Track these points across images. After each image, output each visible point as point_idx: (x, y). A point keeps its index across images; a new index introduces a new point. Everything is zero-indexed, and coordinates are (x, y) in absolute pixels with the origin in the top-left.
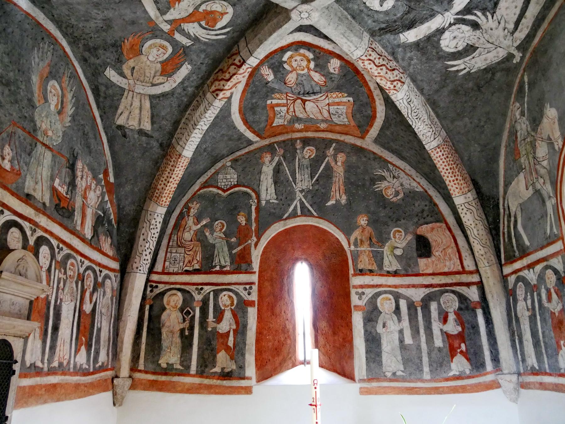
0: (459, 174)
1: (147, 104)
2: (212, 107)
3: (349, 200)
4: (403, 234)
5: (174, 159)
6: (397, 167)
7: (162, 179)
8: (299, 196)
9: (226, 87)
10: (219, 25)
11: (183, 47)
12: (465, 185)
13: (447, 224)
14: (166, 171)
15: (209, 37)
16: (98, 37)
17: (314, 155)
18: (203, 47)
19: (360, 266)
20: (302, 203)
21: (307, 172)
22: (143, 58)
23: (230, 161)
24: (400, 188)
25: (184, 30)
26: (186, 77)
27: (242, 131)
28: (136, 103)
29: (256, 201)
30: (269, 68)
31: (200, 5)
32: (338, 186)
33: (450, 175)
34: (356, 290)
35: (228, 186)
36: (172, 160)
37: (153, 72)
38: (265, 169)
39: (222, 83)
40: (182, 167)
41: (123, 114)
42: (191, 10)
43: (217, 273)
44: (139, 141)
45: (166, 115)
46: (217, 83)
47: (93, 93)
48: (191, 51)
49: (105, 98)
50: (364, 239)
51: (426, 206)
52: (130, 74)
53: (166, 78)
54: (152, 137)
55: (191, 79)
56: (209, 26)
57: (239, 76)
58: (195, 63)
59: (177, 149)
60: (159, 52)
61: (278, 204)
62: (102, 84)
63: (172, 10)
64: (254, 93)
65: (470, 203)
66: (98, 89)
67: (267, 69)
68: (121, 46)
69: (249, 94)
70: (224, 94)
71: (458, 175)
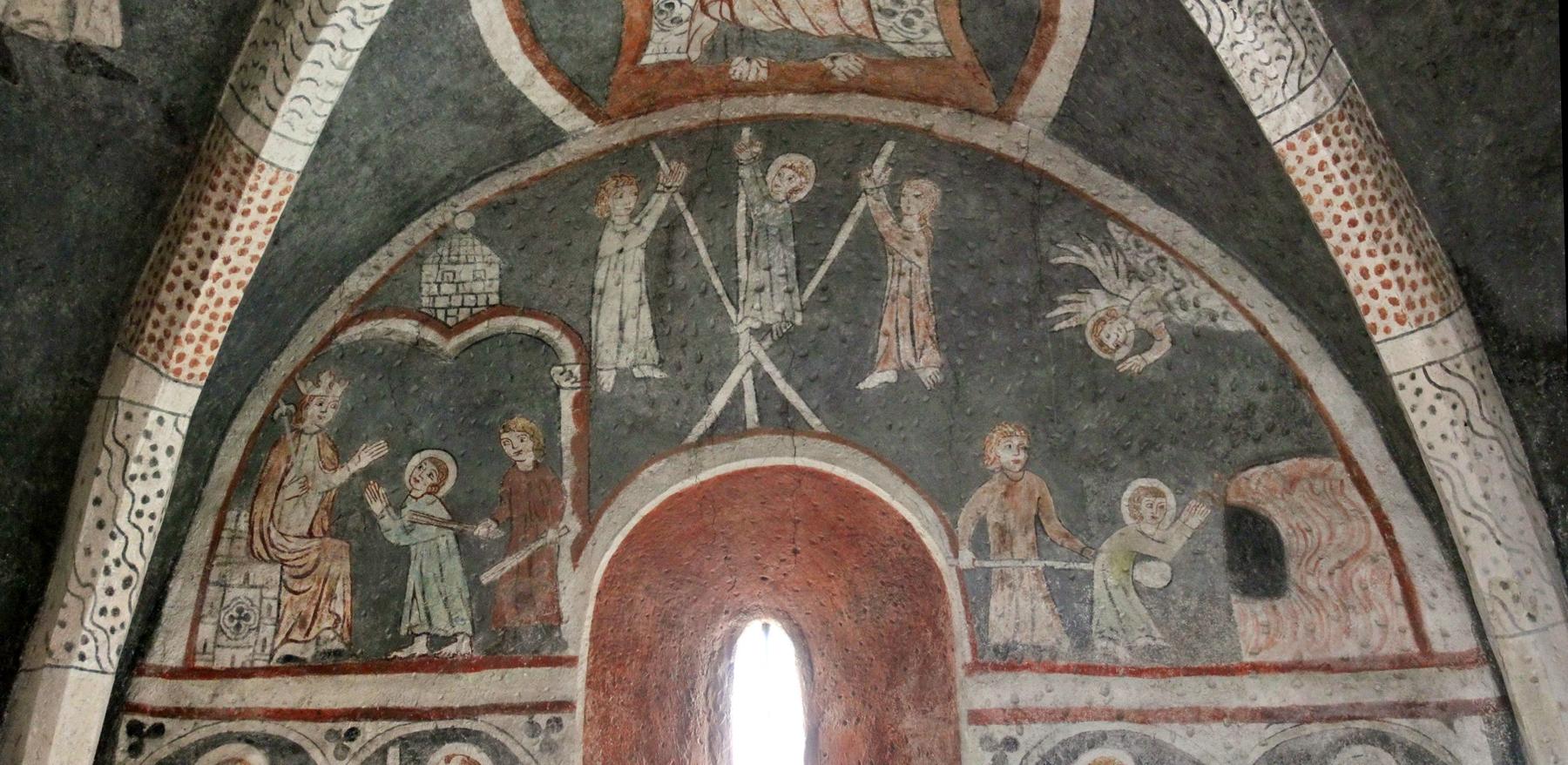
0: (1404, 243)
3: (953, 366)
4: (1171, 500)
5: (226, 175)
6: (1143, 233)
7: (176, 262)
8: (751, 352)
12: (1430, 289)
13: (1350, 463)
14: (195, 228)
17: (808, 188)
19: (1000, 631)
20: (763, 383)
21: (782, 257)
23: (469, 210)
24: (1159, 317)
27: (516, 80)
29: (577, 370)
32: (905, 312)
33: (1363, 247)
34: (981, 730)
35: (464, 314)
36: (220, 182)
38: (610, 242)
40: (262, 210)
43: (409, 666)
44: (73, 94)
50: (1012, 524)
51: (1263, 389)
59: (240, 133)
61: (664, 383)
65: (1450, 365)
71: (1398, 247)
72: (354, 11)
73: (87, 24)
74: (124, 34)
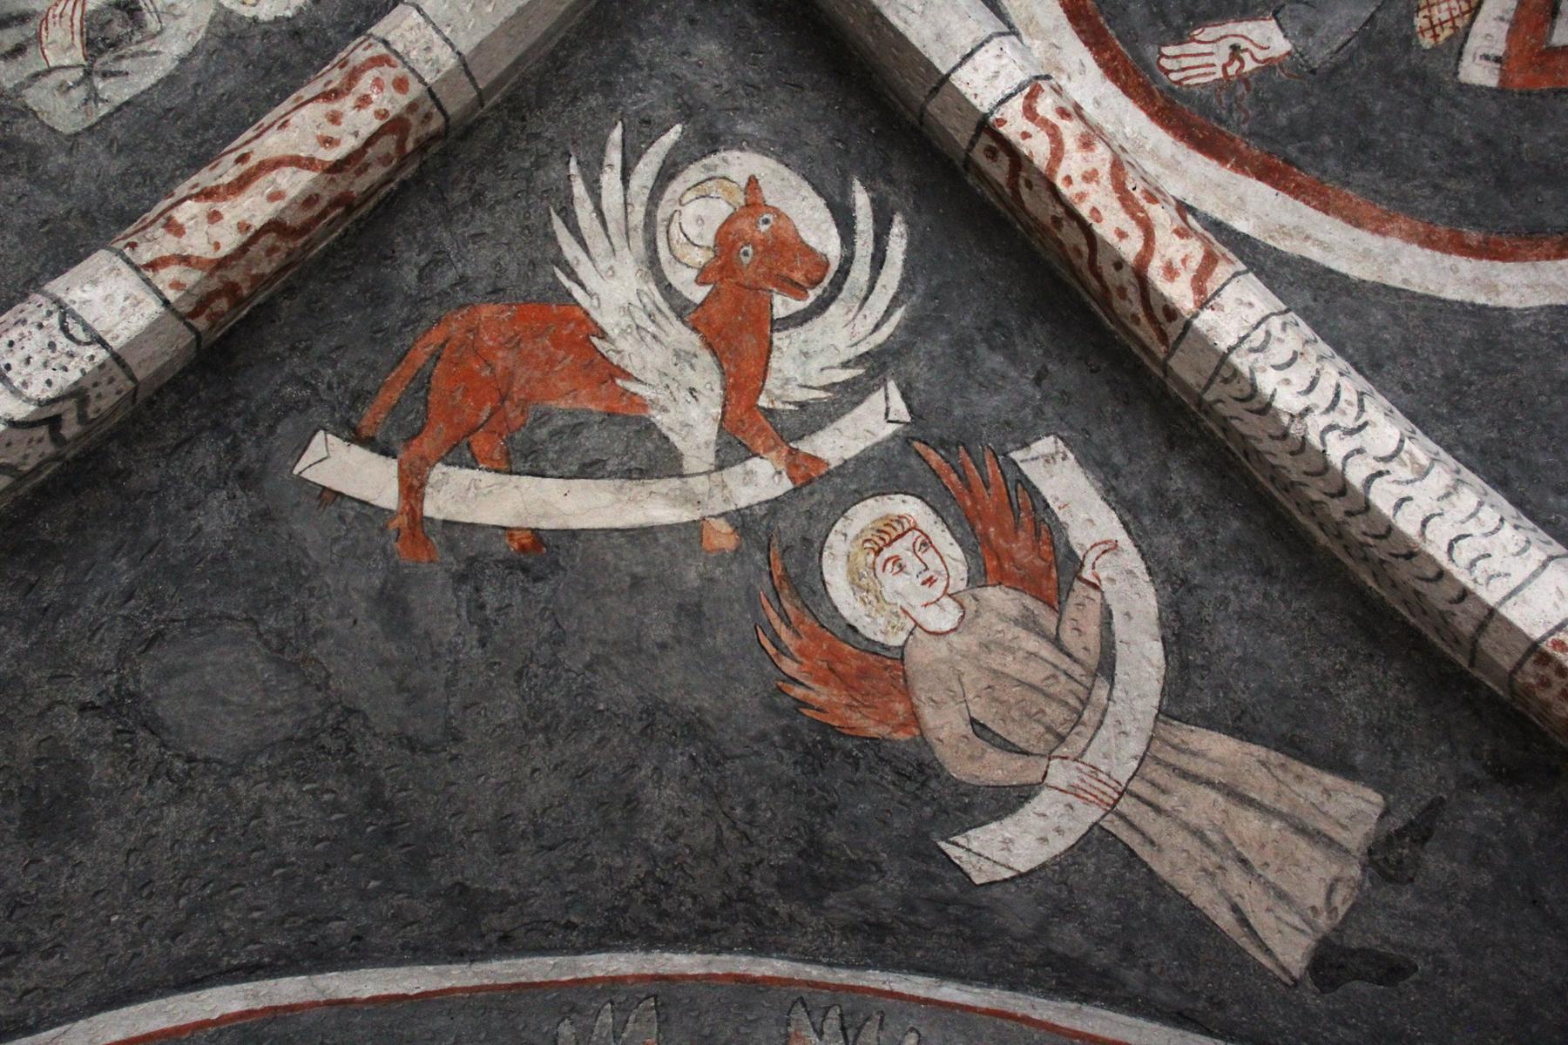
1: (1218, 747)
2: (1241, 361)
9: (1130, 248)
10: (824, 239)
11: (905, 440)
15: (880, 301)
16: (751, 806)
22: (922, 655)
25: (802, 405)
28: (1203, 806)
30: (1180, 38)
31: (667, 290)
37: (1032, 643)
39: (1108, 271)
41: (1246, 907)
42: (681, 335)
45: (1309, 668)
46: (1117, 303)
47: (1086, 998)
48: (948, 412)
49: (1128, 951)
52: (1018, 762)
54: (1434, 808)
56: (814, 284)
57: (1073, 164)
60: (912, 564)
62: (1042, 929)
63: (658, 418)
64: (1365, 147)
66: (1064, 959)
67: (1193, 48)
68: (824, 728)
69: (1359, 177)
70: (1170, 272)
73: (1344, 827)
74: (1366, 785)
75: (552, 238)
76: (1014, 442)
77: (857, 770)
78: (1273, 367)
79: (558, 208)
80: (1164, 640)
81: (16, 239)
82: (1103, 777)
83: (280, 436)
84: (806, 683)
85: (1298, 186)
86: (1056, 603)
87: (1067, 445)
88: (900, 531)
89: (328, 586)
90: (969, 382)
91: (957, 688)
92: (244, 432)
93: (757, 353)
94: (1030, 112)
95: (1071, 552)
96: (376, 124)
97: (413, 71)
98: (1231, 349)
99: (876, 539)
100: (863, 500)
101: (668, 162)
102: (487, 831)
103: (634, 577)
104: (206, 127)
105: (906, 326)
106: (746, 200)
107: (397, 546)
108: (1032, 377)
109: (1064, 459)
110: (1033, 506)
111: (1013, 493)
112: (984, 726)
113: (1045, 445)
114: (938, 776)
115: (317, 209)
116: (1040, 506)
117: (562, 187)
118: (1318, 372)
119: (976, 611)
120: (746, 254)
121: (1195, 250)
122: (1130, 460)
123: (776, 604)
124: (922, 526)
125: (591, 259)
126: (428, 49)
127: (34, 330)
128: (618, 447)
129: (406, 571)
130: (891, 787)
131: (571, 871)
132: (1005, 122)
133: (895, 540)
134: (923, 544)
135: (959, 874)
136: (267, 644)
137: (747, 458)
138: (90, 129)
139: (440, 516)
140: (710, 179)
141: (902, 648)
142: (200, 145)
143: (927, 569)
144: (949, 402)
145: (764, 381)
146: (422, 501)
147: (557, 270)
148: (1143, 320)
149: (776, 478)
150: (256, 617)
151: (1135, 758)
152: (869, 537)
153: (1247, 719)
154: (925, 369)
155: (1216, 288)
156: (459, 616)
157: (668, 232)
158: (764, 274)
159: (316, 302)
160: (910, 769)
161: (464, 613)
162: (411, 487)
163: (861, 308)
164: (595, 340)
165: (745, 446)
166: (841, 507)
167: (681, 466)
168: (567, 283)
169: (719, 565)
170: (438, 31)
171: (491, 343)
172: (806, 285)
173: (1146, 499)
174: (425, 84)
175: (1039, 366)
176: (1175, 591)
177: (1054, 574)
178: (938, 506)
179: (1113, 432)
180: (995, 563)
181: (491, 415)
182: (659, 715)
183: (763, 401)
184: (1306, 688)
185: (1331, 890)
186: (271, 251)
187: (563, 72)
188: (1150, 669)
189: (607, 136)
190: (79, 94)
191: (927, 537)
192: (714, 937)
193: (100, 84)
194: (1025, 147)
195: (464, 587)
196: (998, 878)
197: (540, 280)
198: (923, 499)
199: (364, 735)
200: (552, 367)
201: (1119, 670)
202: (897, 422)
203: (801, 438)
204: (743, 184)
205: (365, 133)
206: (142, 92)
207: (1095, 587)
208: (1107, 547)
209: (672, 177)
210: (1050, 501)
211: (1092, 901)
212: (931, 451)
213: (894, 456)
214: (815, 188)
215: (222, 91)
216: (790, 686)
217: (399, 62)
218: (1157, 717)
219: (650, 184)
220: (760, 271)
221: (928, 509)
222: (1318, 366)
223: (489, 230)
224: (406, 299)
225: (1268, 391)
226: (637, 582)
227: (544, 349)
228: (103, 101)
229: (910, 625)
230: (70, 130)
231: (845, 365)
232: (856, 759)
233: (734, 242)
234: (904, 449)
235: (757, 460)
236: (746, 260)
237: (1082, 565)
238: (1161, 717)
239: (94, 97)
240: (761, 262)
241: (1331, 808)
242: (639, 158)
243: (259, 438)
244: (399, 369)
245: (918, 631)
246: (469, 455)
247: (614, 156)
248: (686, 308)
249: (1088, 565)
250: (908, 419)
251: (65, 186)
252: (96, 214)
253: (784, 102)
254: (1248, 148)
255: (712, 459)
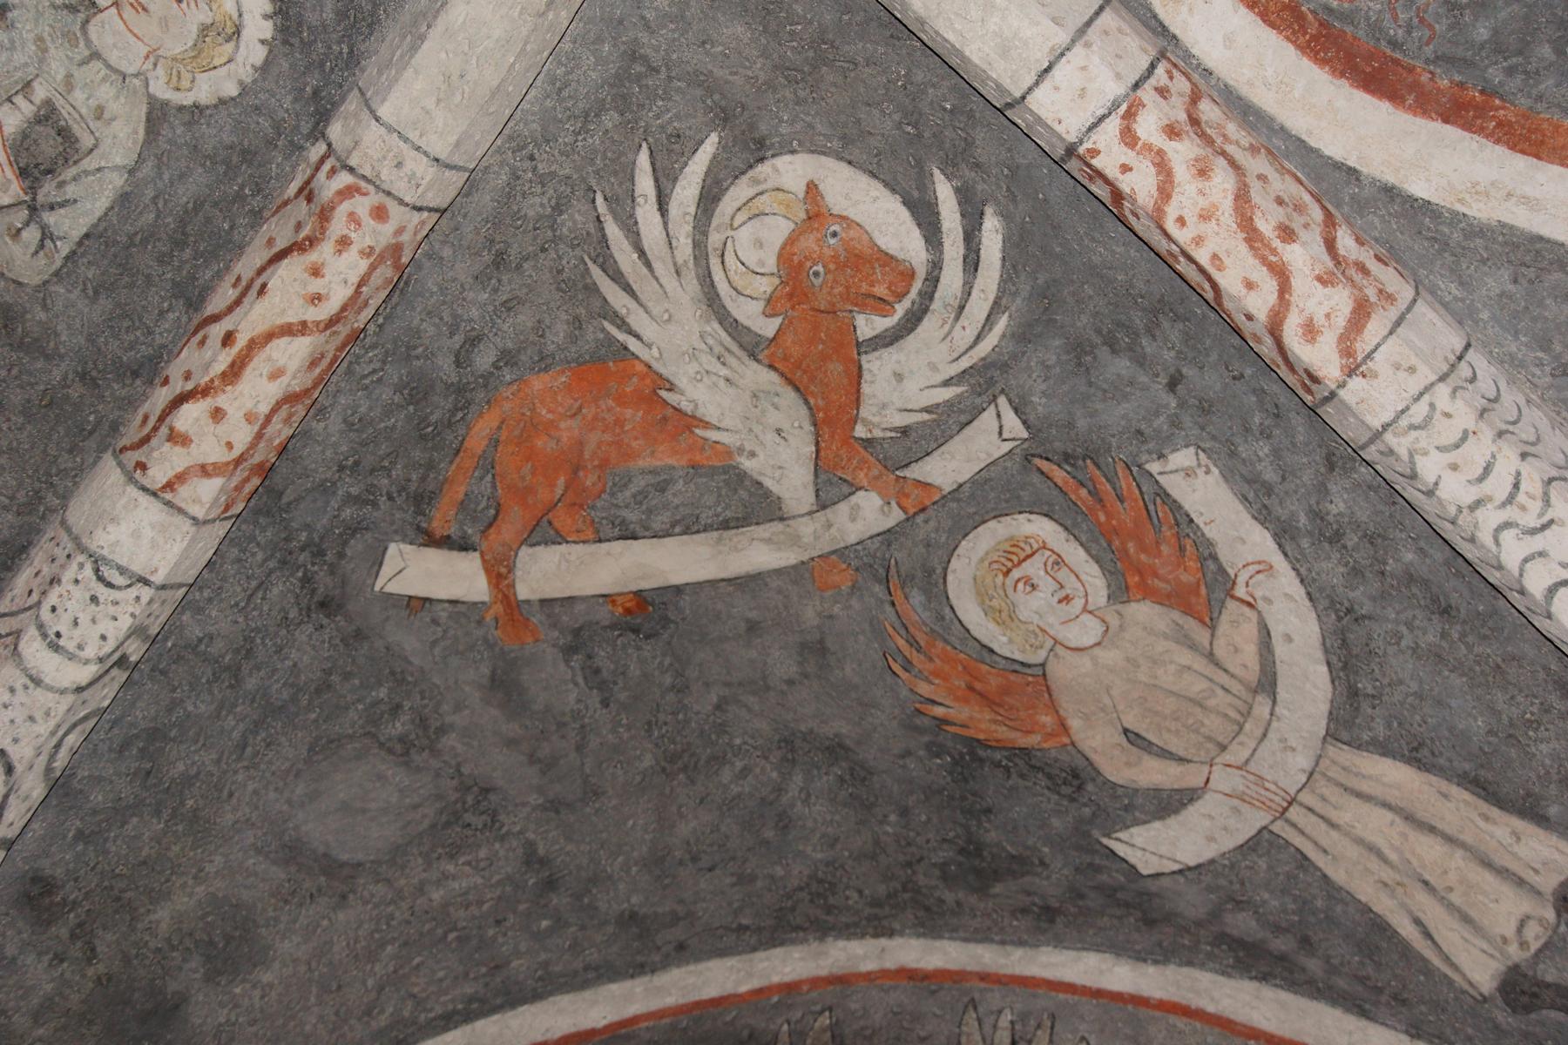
1: (1394, 775)
9: (1260, 303)
11: (1028, 456)
15: (979, 307)
18: (1051, 351)
22: (1063, 671)
25: (905, 431)
26: (1244, 499)
28: (1376, 825)
37: (1185, 657)
48: (1071, 425)
49: (1305, 942)
53: (1231, 605)
55: (1270, 475)
56: (901, 296)
57: (1188, 196)
58: (1161, 422)
62: (1216, 914)
63: (747, 464)
70: (1310, 331)
72: (1507, 525)
73: (1536, 871)
75: (593, 289)
76: (1149, 452)
77: (1009, 777)
78: (1438, 448)
79: (593, 254)
80: (1329, 664)
81: (21, 420)
82: (1267, 785)
83: (352, 558)
84: (940, 700)
85: (1500, 124)
86: (1207, 620)
87: (1209, 458)
88: (1029, 551)
89: (438, 687)
90: (1092, 390)
91: (1107, 701)
92: (313, 564)
93: (845, 381)
94: (1128, 137)
95: (1222, 570)
96: (364, 265)
97: (389, 194)
98: (1385, 427)
99: (1003, 560)
100: (984, 522)
101: (709, 181)
102: (645, 865)
103: (748, 621)
104: (180, 244)
105: (1013, 335)
106: (807, 211)
107: (498, 633)
108: (1165, 381)
109: (1208, 472)
110: (1176, 520)
111: (1151, 507)
112: (1137, 735)
113: (1183, 458)
114: (1093, 780)
115: (325, 363)
116: (1183, 520)
117: (593, 231)
118: (1494, 456)
119: (1121, 626)
120: (816, 274)
121: (1340, 301)
122: (1284, 478)
123: (903, 632)
124: (1051, 544)
125: (641, 305)
126: (399, 165)
127: (71, 587)
128: (709, 500)
129: (513, 655)
130: (1046, 791)
131: (734, 885)
132: (1099, 152)
133: (1024, 560)
134: (1057, 563)
135: (1125, 865)
136: (390, 751)
137: (851, 494)
138: (57, 274)
139: (535, 597)
140: (761, 193)
141: (1043, 665)
142: (180, 268)
143: (1062, 587)
144: (1070, 413)
145: (858, 409)
146: (514, 587)
147: (606, 324)
148: (1283, 367)
149: (886, 509)
150: (373, 730)
151: (1304, 771)
152: (996, 558)
153: (1425, 752)
154: (1039, 381)
155: (1368, 349)
156: (576, 684)
157: (723, 263)
158: (840, 294)
159: (352, 415)
160: (1064, 775)
161: (580, 680)
162: (500, 576)
163: (957, 318)
164: (663, 394)
165: (845, 481)
166: (964, 528)
167: (780, 509)
168: (622, 337)
169: (836, 602)
170: (406, 140)
171: (550, 416)
172: (891, 299)
173: (1303, 520)
174: (407, 205)
175: (1172, 370)
176: (1340, 619)
177: (1203, 591)
178: (1069, 523)
179: (1264, 449)
180: (1137, 579)
181: (567, 488)
182: (798, 743)
183: (860, 431)
184: (1490, 732)
185: (1522, 924)
186: (287, 421)
187: (565, 93)
188: (1315, 692)
189: (634, 163)
190: (31, 235)
191: (1059, 556)
192: (885, 923)
193: (50, 218)
194: (1125, 183)
195: (575, 657)
196: (1167, 870)
197: (590, 337)
198: (1051, 518)
199: (506, 807)
200: (622, 427)
201: (1280, 689)
202: (1013, 439)
203: (907, 465)
204: (801, 195)
205: (354, 279)
206: (99, 220)
207: (1249, 605)
208: (1261, 567)
209: (716, 199)
210: (1193, 516)
211: (1266, 896)
212: (1055, 467)
213: (1013, 476)
214: (886, 184)
215: (185, 199)
216: (930, 707)
217: (371, 188)
218: (1324, 738)
219: (692, 210)
220: (836, 291)
221: (1060, 529)
222: (1494, 449)
223: (522, 293)
224: (447, 389)
225: (1431, 479)
226: (753, 627)
227: (609, 410)
228: (60, 238)
229: (1050, 643)
230: (37, 280)
231: (947, 383)
232: (1007, 769)
233: (801, 264)
234: (1025, 467)
235: (861, 493)
236: (817, 282)
237: (1234, 583)
238: (1329, 738)
239: (46, 235)
240: (835, 281)
241: (1522, 850)
242: (675, 180)
243: (331, 565)
244: (458, 460)
245: (1059, 649)
246: (552, 532)
247: (645, 184)
248: (758, 344)
249: (1241, 580)
250: (1025, 435)
251: (52, 344)
252: (94, 373)
253: (835, 85)
254: (1431, 79)
255: (811, 498)
